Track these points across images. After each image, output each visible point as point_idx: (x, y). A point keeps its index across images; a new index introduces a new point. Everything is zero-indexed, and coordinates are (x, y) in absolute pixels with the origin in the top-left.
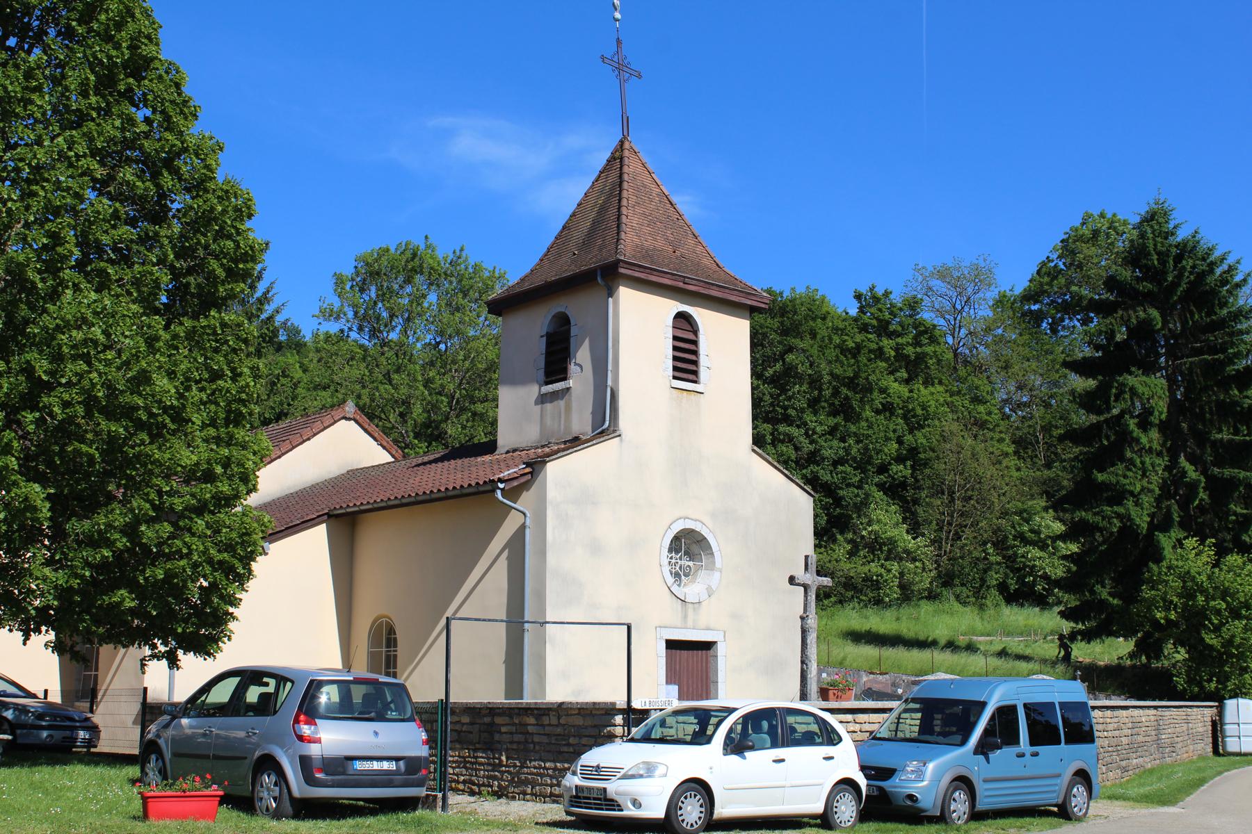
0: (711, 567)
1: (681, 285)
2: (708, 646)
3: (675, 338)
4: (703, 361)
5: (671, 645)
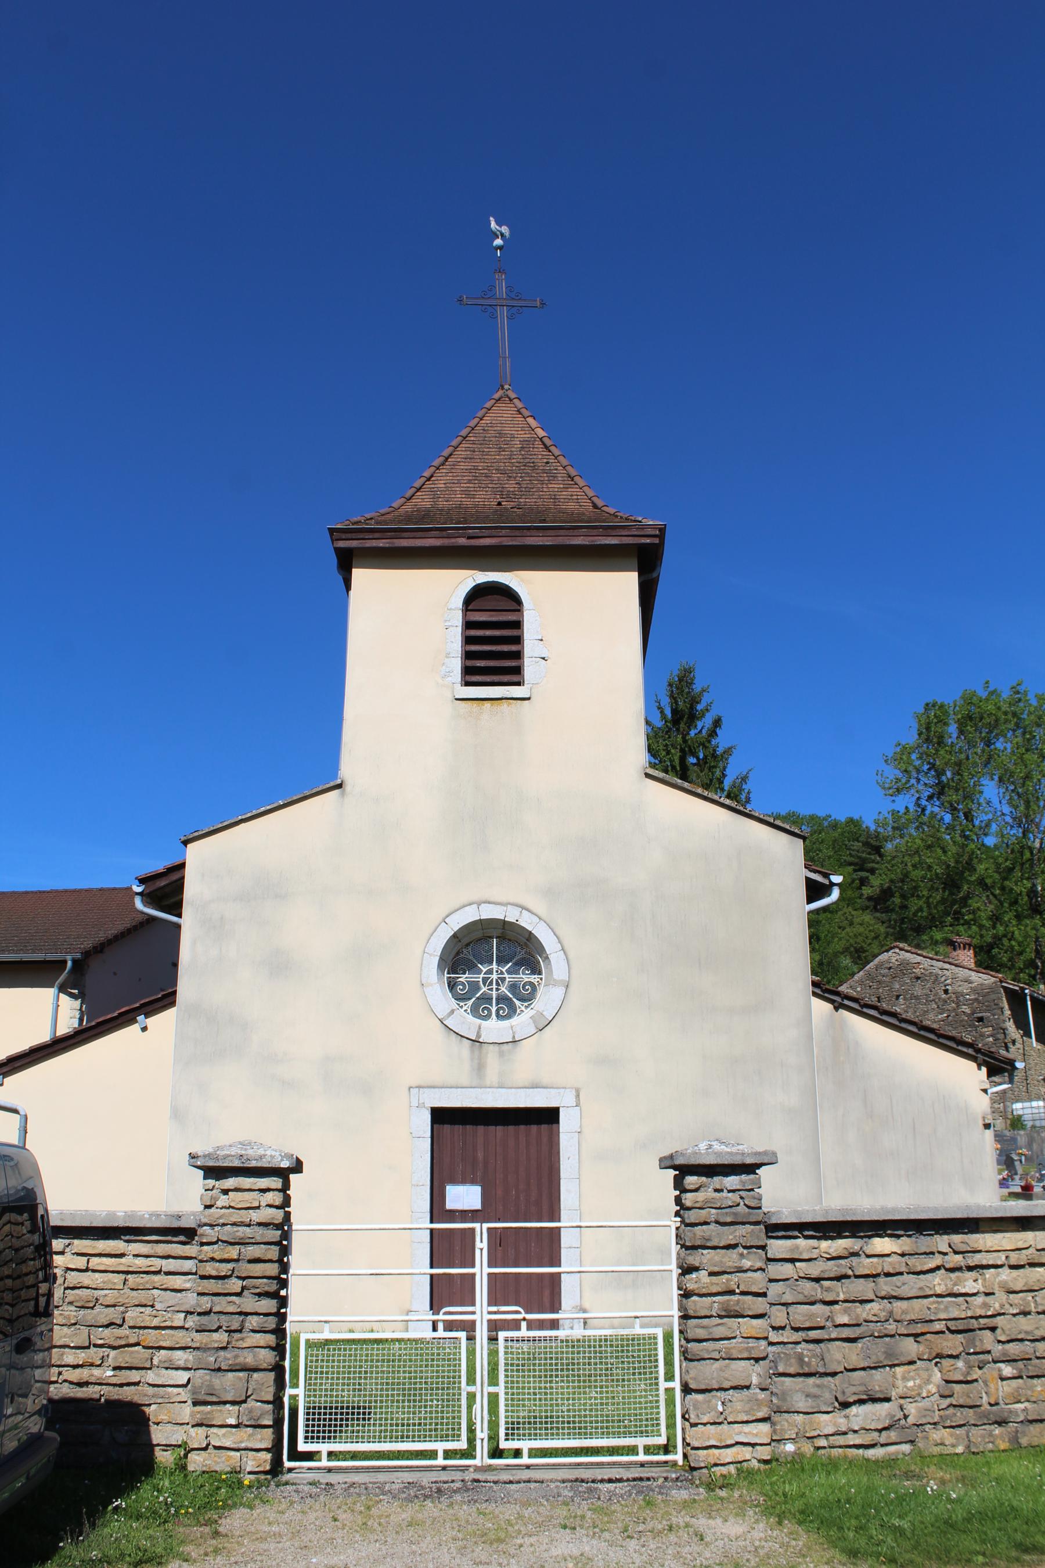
0: (552, 983)
1: (462, 541)
2: (550, 1116)
3: (468, 625)
4: (530, 647)
5: (441, 1116)
